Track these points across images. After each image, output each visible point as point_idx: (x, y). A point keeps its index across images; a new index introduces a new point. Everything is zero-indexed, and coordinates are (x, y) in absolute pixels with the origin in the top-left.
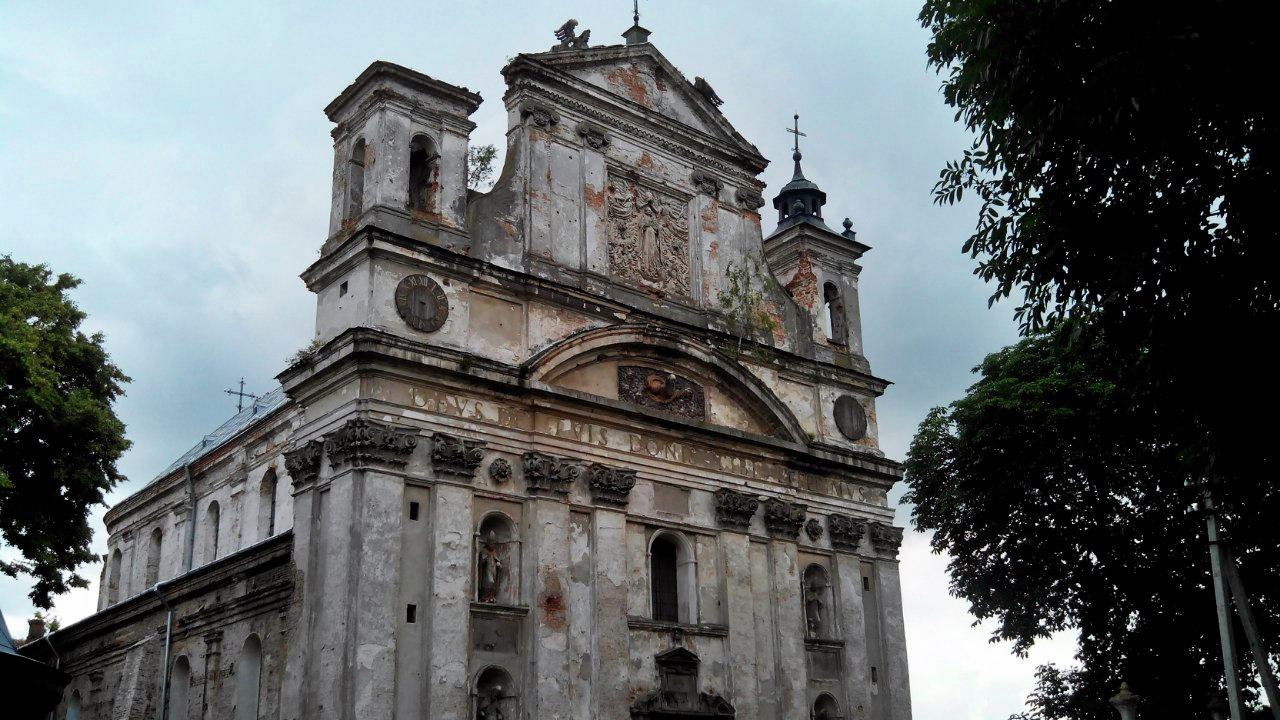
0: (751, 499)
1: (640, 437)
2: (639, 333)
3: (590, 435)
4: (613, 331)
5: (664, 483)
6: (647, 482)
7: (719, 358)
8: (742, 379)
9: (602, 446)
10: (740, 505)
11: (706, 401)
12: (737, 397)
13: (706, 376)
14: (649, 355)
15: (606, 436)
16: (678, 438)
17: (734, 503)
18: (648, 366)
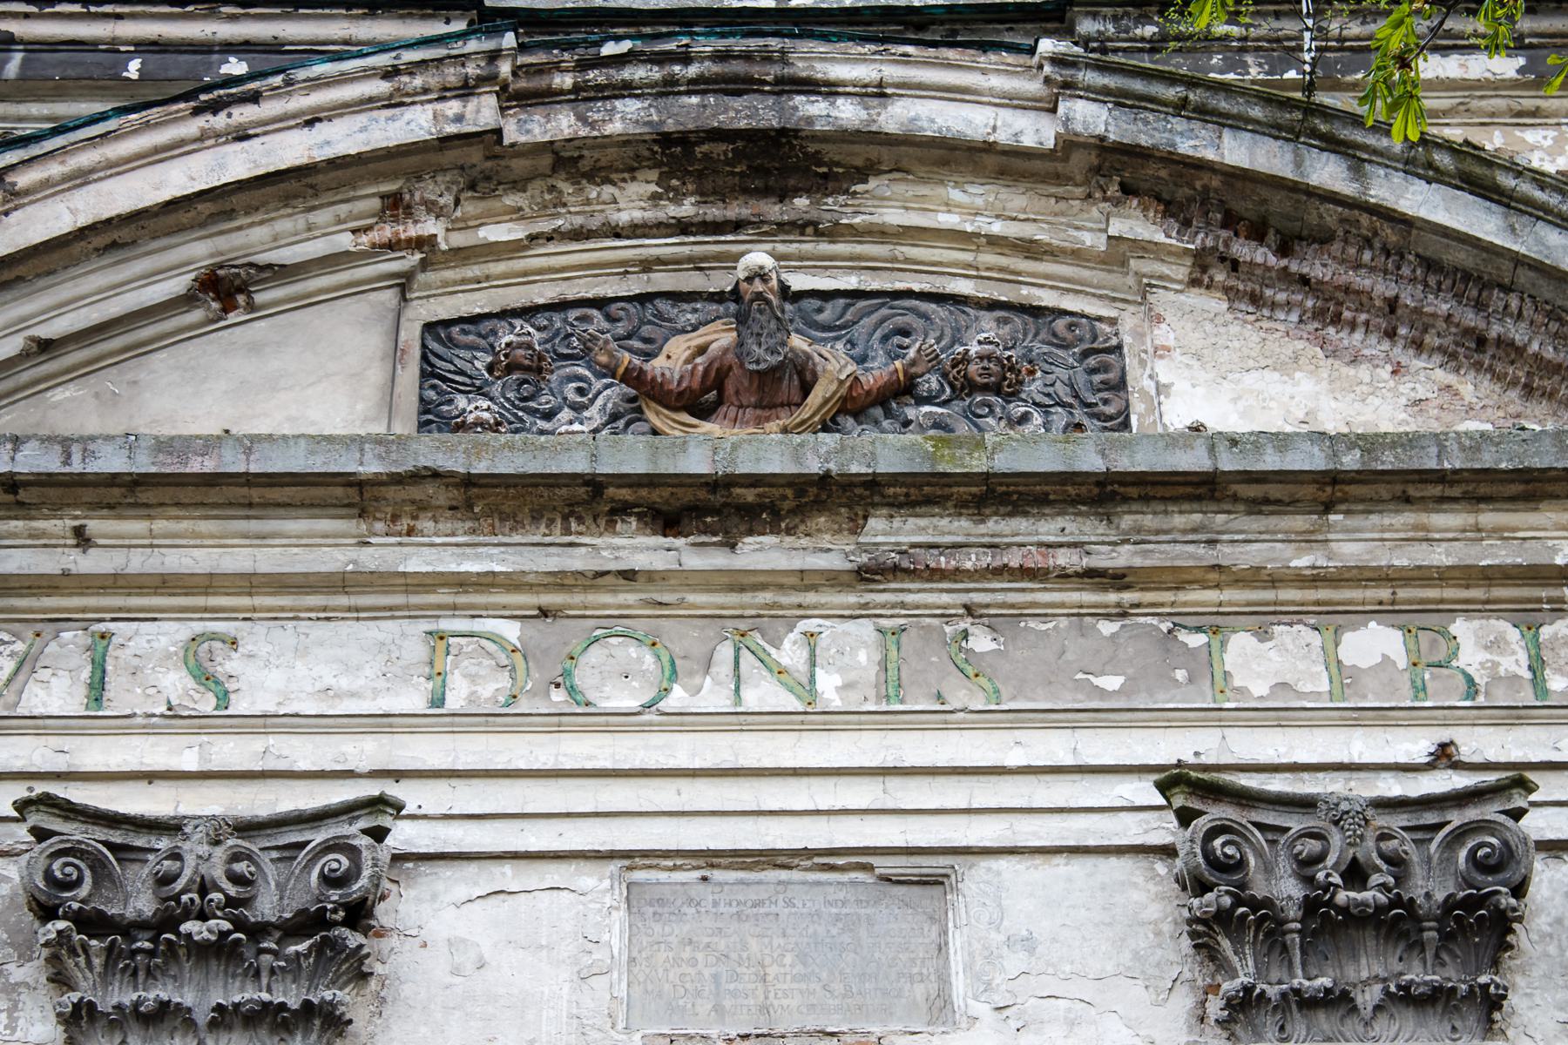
0: (1456, 818)
1: (511, 631)
2: (466, 90)
3: (97, 688)
4: (243, 114)
5: (710, 858)
6: (555, 873)
7: (1119, 99)
8: (1327, 172)
9: (174, 719)
10: (1355, 874)
11: (1138, 380)
12: (1362, 299)
13: (1092, 240)
14: (623, 218)
15: (228, 664)
16: (806, 580)
17: (1305, 866)
18: (663, 281)
